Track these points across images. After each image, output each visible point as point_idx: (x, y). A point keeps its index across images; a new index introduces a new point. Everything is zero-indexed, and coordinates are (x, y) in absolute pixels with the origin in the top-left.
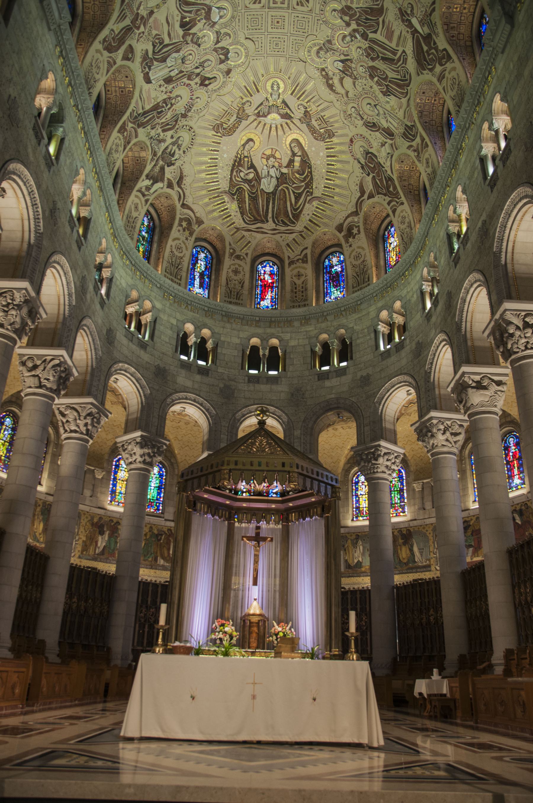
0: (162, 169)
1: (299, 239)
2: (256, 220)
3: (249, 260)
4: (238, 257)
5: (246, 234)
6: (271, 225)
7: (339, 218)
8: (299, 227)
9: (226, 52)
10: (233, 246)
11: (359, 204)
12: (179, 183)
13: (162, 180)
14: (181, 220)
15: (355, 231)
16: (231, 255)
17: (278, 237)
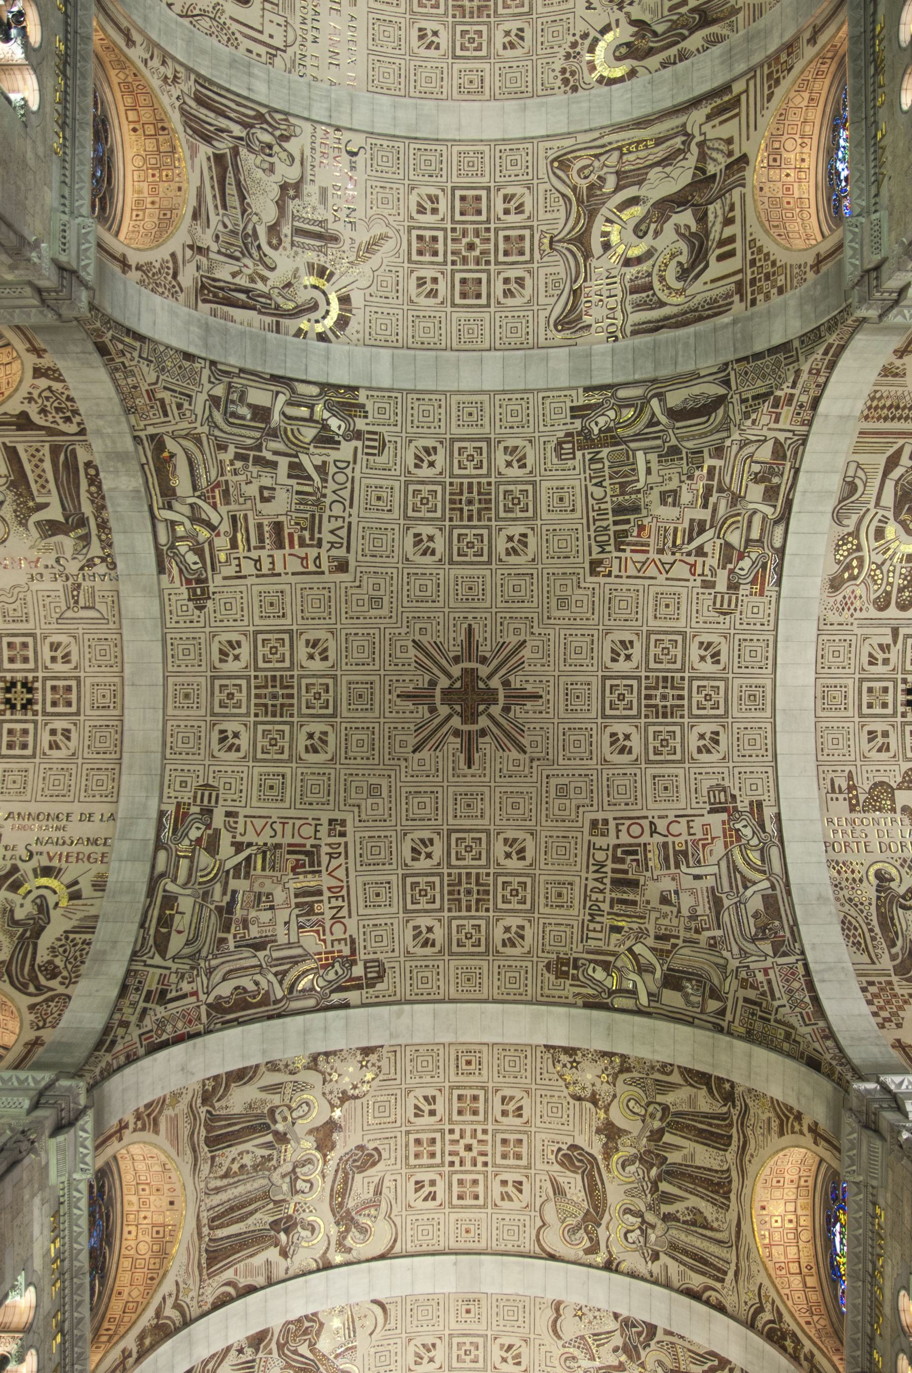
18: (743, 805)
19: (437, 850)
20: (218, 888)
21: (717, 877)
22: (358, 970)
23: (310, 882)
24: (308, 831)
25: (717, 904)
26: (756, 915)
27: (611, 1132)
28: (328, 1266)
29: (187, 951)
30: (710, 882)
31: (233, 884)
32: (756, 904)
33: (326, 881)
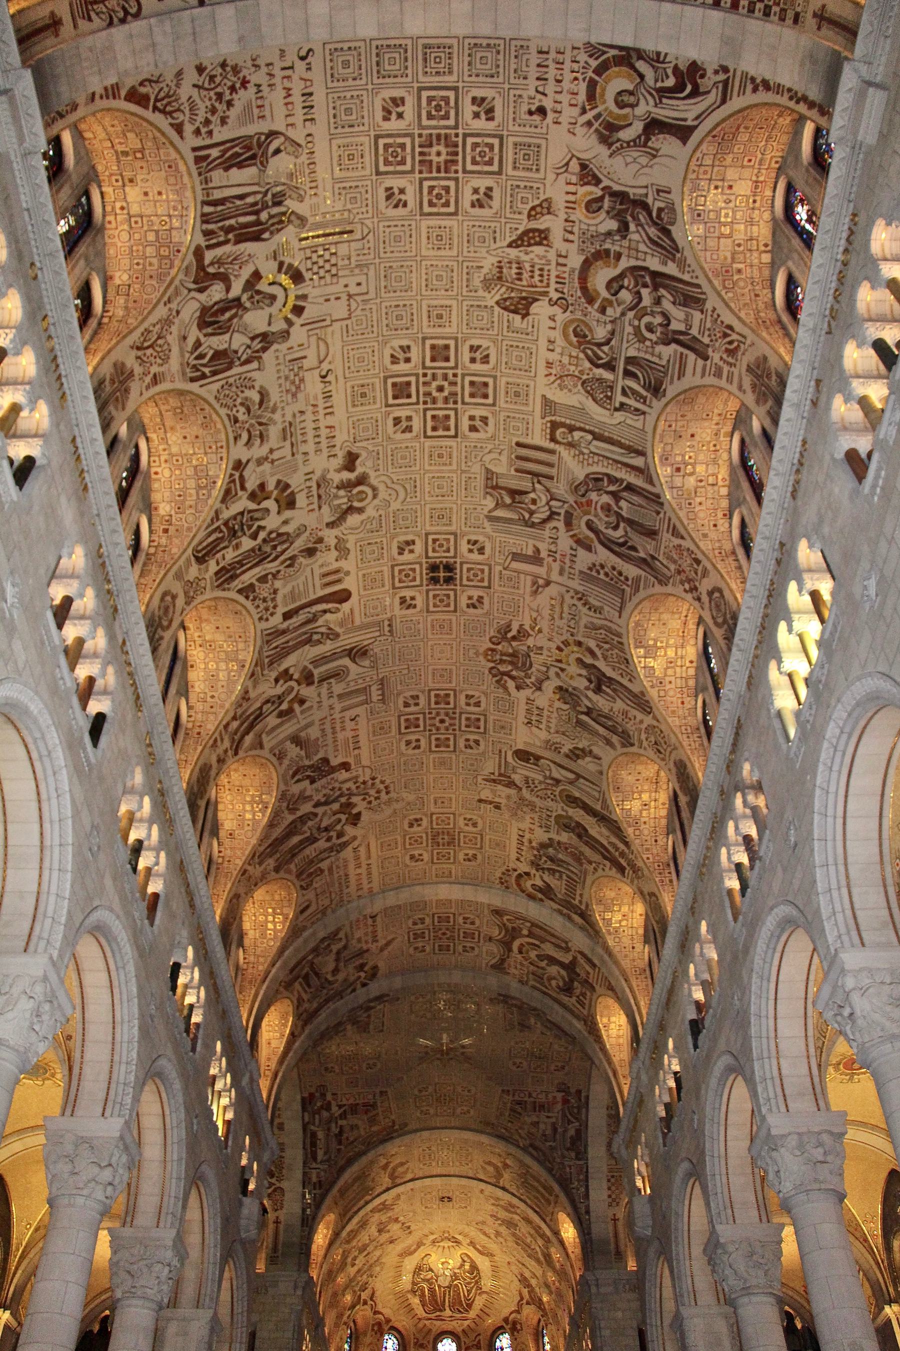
0: (360, 1296)
1: (473, 1325)
2: (435, 1310)
3: (430, 1346)
4: (422, 1346)
5: (427, 1322)
6: (448, 1312)
7: (505, 1312)
8: (472, 1314)
9: (409, 1227)
10: (417, 1336)
11: (520, 1305)
12: (371, 1299)
13: (358, 1303)
14: (373, 1325)
15: (518, 1327)
16: (415, 1344)
17: (454, 1323)
18: (573, 1090)
19: (431, 1089)
20: (333, 1125)
21: (557, 1118)
22: (397, 1127)
23: (374, 1112)
24: (370, 1097)
25: (555, 1130)
26: (571, 1137)
27: (506, 1166)
28: (388, 1189)
29: (325, 1158)
30: (554, 1120)
31: (340, 1122)
32: (572, 1132)
33: (380, 1109)
